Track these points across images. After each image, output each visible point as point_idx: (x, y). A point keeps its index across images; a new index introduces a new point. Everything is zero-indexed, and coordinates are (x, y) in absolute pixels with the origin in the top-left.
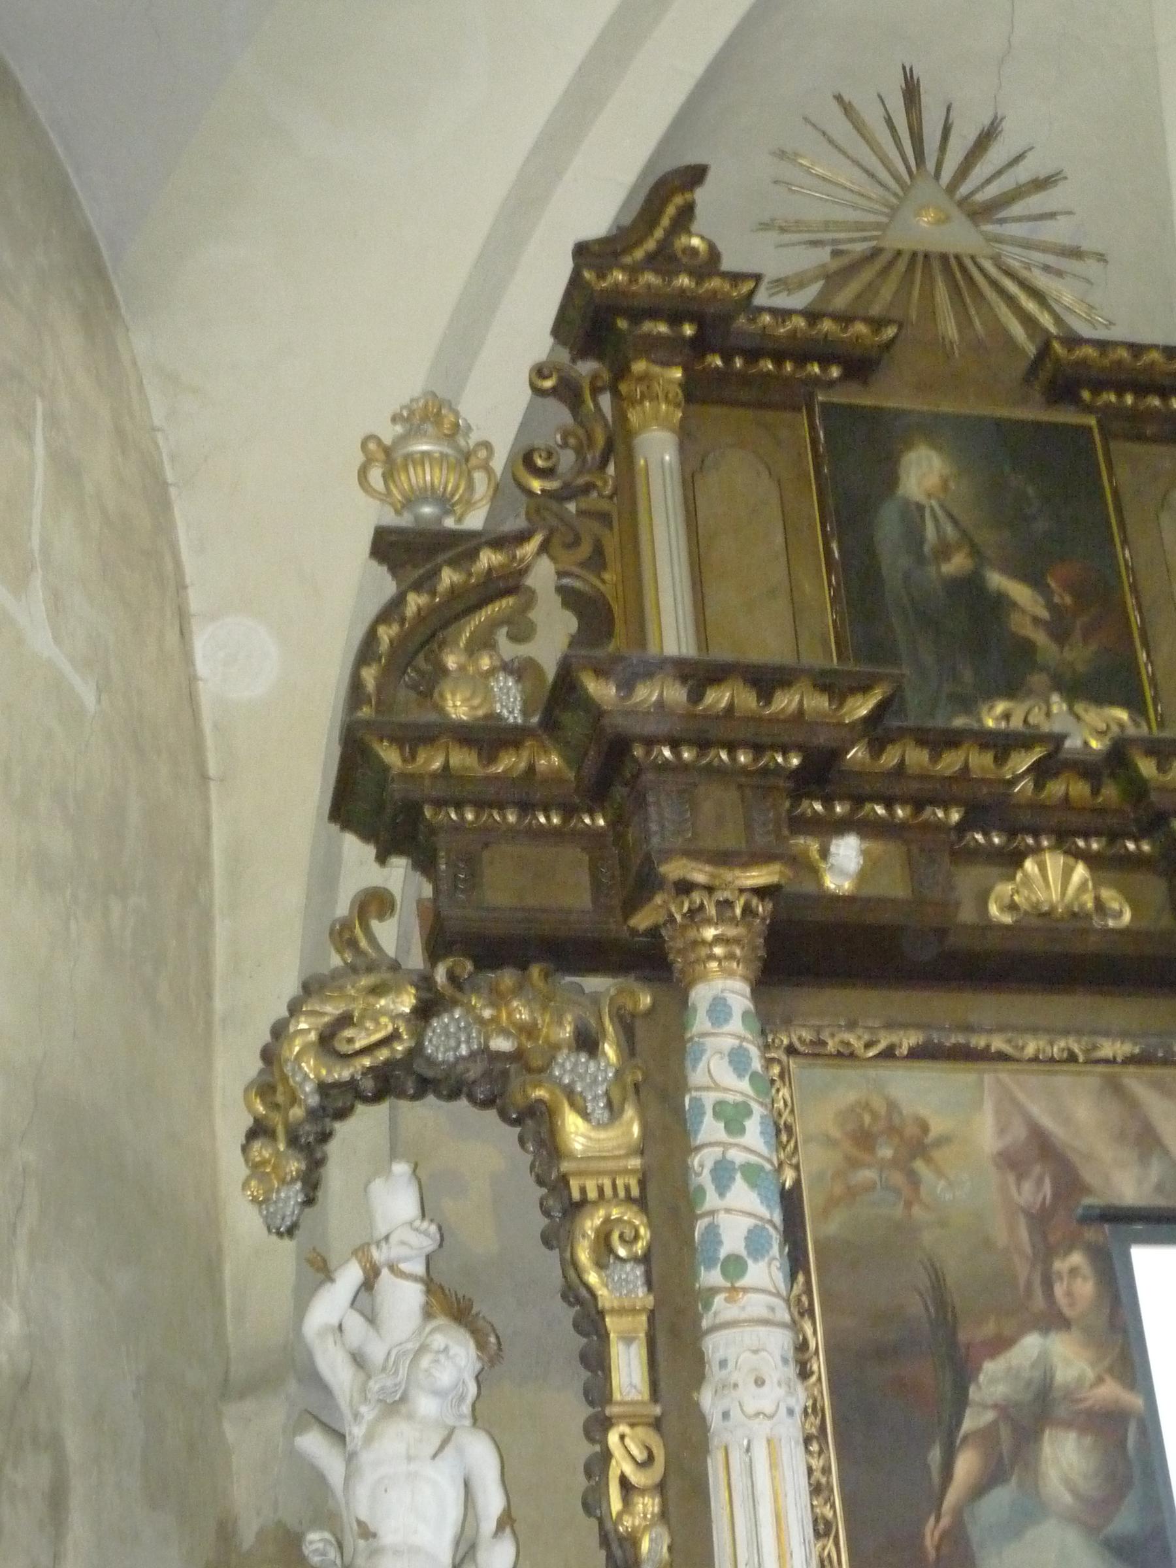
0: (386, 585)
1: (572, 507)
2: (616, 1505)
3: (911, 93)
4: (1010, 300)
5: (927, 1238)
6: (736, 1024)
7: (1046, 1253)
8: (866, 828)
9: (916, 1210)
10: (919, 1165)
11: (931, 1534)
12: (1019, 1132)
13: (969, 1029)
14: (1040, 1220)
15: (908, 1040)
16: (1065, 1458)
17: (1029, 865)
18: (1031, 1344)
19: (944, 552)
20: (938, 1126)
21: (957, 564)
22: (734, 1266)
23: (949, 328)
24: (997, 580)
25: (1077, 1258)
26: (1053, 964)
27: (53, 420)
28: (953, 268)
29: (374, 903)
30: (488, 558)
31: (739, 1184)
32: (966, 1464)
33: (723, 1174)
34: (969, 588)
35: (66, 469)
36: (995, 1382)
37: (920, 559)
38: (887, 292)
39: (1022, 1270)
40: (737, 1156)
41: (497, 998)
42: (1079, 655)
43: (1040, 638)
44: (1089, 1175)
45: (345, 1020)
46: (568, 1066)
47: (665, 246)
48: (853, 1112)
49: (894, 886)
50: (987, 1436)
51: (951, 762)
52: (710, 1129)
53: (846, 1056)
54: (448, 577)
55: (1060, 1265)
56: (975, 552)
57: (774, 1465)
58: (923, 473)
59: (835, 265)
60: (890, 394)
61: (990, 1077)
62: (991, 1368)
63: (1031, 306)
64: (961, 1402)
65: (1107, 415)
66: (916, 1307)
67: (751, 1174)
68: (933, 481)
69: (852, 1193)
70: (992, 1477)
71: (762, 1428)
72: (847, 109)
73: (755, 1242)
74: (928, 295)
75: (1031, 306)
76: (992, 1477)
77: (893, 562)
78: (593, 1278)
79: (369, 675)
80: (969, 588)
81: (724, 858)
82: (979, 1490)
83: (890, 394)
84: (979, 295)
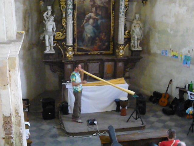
2: (62, 23)
5: (84, 6)
9: (84, 5)
10: (84, 2)
11: (82, 25)
14: (92, 5)
16: (91, 21)
18: (90, 13)
22: (69, 15)
25: (94, 8)
31: (70, 10)
32: (85, 21)
33: (69, 9)
36: (87, 16)
39: (90, 9)
40: (70, 8)
44: (96, 2)
50: (86, 20)
52: (68, 6)
55: (93, 8)
57: (70, 27)
62: (87, 15)
64: (85, 17)
67: (71, 9)
70: (86, 22)
71: (70, 25)
73: (70, 13)
76: (86, 22)
78: (62, 10)
82: (85, 23)
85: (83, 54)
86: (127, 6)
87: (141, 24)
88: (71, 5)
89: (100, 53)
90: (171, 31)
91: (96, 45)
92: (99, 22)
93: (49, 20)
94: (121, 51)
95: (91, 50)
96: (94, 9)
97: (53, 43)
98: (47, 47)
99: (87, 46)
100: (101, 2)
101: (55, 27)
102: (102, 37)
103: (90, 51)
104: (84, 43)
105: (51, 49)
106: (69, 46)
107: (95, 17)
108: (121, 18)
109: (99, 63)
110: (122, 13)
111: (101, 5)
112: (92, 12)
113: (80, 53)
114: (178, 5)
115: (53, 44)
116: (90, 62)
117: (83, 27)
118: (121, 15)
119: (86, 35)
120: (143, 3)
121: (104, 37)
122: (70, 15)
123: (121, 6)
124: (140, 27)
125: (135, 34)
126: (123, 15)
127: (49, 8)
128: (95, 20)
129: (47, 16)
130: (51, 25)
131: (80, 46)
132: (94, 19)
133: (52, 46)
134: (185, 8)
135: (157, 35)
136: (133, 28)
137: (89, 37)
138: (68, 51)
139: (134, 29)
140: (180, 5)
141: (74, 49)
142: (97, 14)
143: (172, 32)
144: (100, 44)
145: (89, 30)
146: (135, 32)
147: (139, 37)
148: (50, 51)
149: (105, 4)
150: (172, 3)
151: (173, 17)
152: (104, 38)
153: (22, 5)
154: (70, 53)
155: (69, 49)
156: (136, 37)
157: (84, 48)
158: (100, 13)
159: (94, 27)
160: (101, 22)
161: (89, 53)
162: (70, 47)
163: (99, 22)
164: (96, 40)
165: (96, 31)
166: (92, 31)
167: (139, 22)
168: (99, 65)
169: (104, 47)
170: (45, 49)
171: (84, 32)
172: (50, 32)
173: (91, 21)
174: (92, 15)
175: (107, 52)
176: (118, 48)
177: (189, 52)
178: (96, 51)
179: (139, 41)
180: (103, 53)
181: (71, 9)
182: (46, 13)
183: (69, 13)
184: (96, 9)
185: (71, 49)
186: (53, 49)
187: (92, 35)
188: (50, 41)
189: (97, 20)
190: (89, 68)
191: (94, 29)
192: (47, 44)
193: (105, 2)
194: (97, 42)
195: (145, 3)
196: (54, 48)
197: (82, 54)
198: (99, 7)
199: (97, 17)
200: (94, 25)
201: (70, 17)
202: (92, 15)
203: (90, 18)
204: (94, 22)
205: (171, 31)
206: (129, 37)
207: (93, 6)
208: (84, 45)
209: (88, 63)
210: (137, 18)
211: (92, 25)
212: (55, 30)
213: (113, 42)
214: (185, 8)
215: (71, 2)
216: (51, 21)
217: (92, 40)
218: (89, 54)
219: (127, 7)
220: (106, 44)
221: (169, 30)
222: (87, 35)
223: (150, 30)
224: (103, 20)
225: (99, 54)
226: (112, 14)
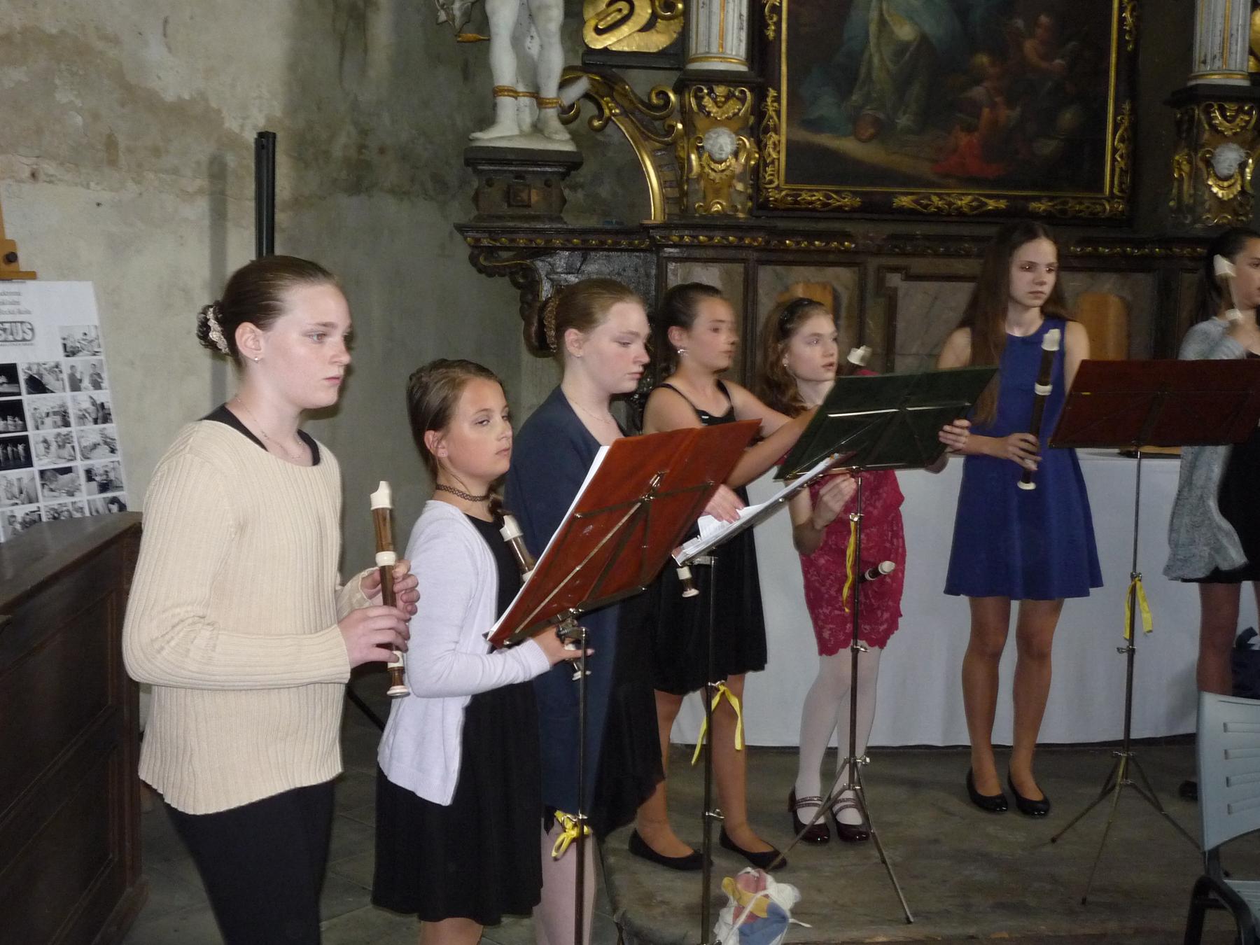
89: (1002, 204)
91: (970, 129)
94: (1228, 157)
95: (924, 169)
98: (498, 92)
99: (883, 131)
102: (1029, 46)
103: (908, 181)
104: (855, 98)
106: (713, 79)
113: (814, 195)
115: (563, 85)
116: (919, 265)
119: (873, 28)
131: (815, 125)
133: (550, 90)
137: (902, 48)
138: (700, 122)
141: (759, 112)
144: (1009, 115)
148: (522, 134)
152: (1044, 65)
154: (723, 142)
155: (707, 102)
157: (848, 145)
161: (905, 201)
162: (720, 90)
169: (1048, 147)
170: (487, 119)
175: (1078, 203)
176: (1189, 136)
186: (555, 124)
188: (533, 47)
190: (900, 325)
192: (505, 67)
194: (978, 92)
197: (836, 201)
208: (853, 123)
209: (895, 280)
213: (1127, 106)
218: (901, 210)
220: (1068, 118)
222: (883, 23)
225: (997, 213)
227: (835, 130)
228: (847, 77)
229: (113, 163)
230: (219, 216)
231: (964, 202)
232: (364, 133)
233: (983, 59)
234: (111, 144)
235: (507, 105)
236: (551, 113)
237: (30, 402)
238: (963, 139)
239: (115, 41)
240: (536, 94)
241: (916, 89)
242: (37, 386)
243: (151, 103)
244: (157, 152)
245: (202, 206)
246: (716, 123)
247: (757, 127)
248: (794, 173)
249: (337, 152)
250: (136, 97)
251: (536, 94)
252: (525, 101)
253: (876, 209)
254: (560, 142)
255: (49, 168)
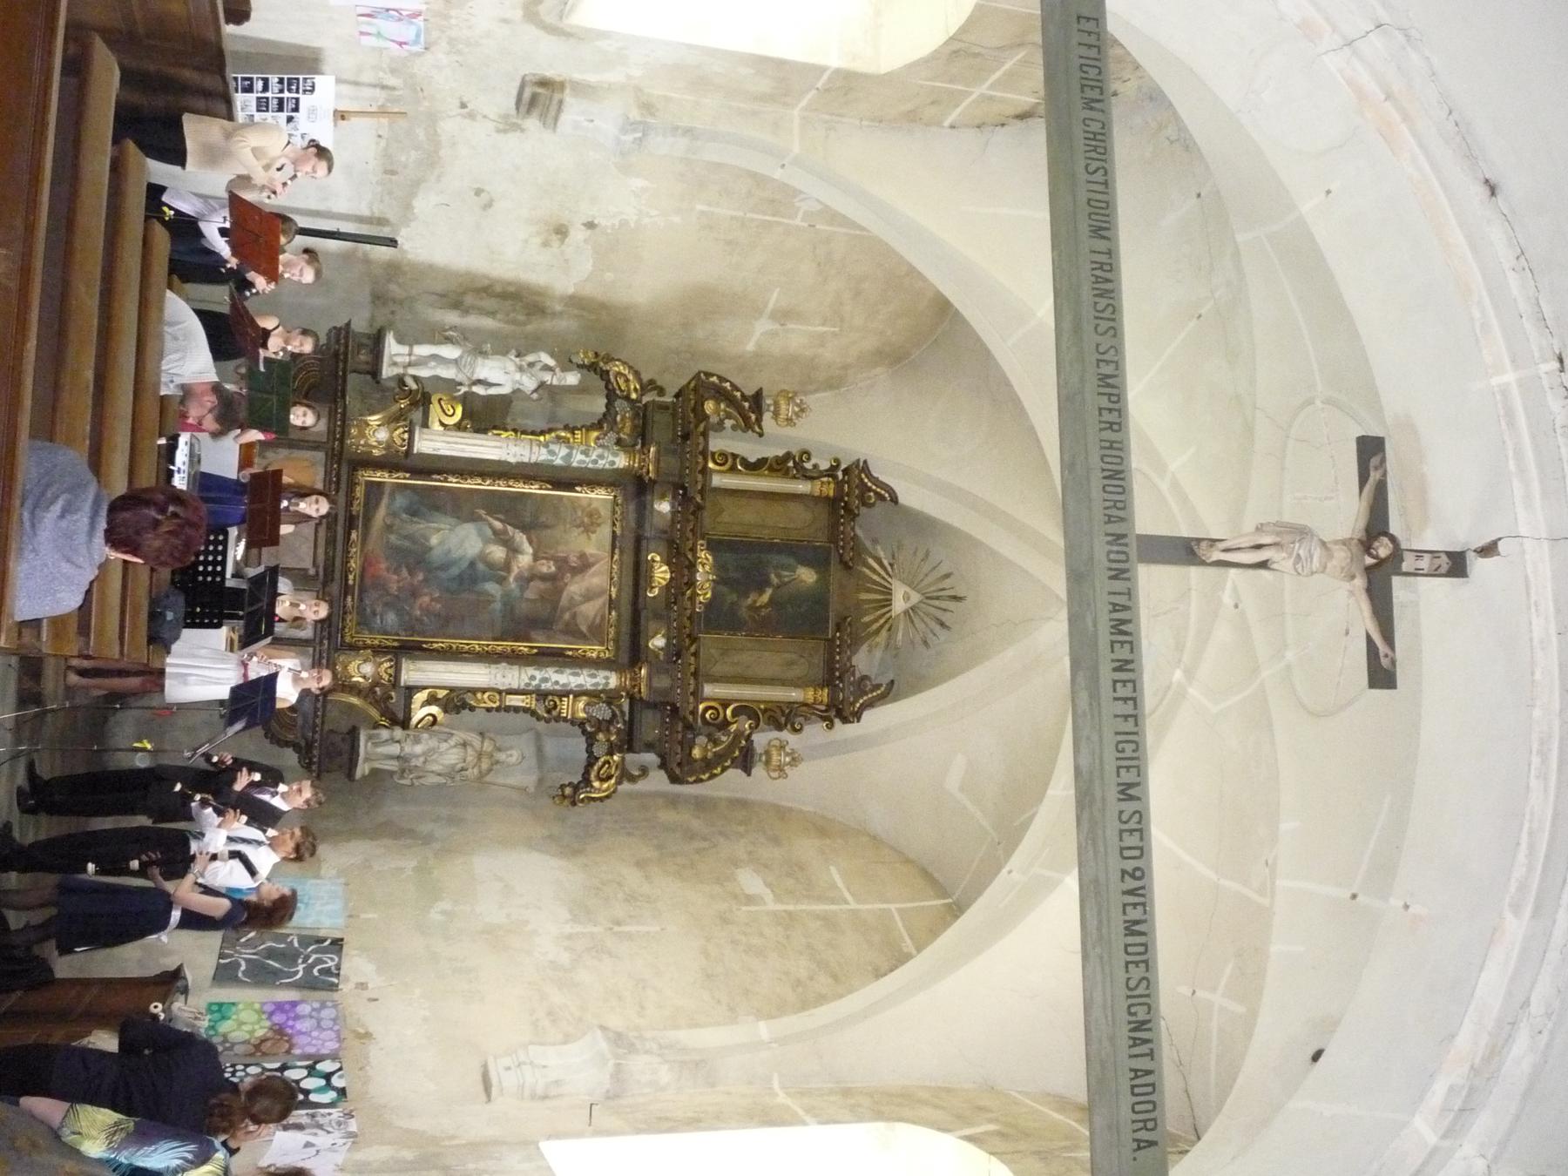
0: (749, 392)
1: (791, 464)
3: (955, 598)
4: (876, 620)
6: (611, 458)
7: (556, 560)
8: (674, 513)
11: (482, 512)
12: (591, 560)
13: (621, 553)
14: (565, 560)
15: (618, 532)
16: (498, 553)
17: (665, 568)
18: (530, 550)
19: (779, 576)
20: (593, 536)
21: (775, 580)
23: (864, 596)
24: (769, 592)
26: (639, 573)
27: (834, 334)
28: (887, 603)
29: (661, 391)
30: (753, 417)
32: (498, 525)
34: (767, 583)
35: (821, 340)
36: (520, 538)
37: (776, 567)
38: (875, 577)
41: (633, 419)
42: (744, 613)
43: (749, 601)
44: (578, 578)
45: (627, 381)
46: (612, 436)
47: (870, 490)
48: (598, 512)
49: (656, 521)
50: (505, 532)
51: (690, 535)
53: (614, 512)
54: (747, 405)
56: (779, 587)
58: (807, 576)
59: (886, 562)
60: (835, 569)
61: (607, 555)
63: (875, 627)
64: (516, 527)
65: (832, 641)
66: (543, 519)
67: (569, 455)
68: (804, 577)
69: (574, 509)
70: (495, 532)
72: (947, 576)
73: (552, 453)
74: (876, 592)
75: (875, 627)
76: (495, 532)
77: (776, 559)
79: (714, 379)
80: (767, 583)
81: (658, 461)
82: (491, 527)
83: (835, 569)
84: (877, 609)
85: (355, 509)
86: (554, 713)
87: (476, 771)
88: (582, 457)
90: (444, 912)
91: (388, 570)
92: (492, 588)
93: (521, 369)
94: (368, 669)
96: (547, 568)
97: (424, 373)
98: (411, 346)
99: (389, 528)
100: (577, 598)
101: (493, 391)
102: (426, 599)
105: (395, 364)
106: (411, 432)
107: (515, 570)
108: (516, 673)
109: (312, 572)
110: (539, 674)
111: (564, 601)
112: (536, 558)
113: (360, 492)
114: (568, 929)
117: (473, 518)
118: (531, 671)
120: (562, 787)
121: (427, 611)
122: (544, 450)
123: (568, 671)
124: (463, 769)
125: (433, 743)
126: (533, 678)
127: (572, 379)
128: (499, 572)
129: (538, 366)
130: (500, 375)
132: (507, 566)
133: (411, 371)
134: (565, 958)
135: (409, 863)
136: (460, 736)
139: (452, 742)
140: (570, 937)
142: (527, 579)
143: (435, 915)
144: (394, 588)
145: (461, 540)
146: (444, 746)
147: (419, 762)
149: (567, 616)
150: (570, 911)
151: (508, 916)
153: (571, 290)
154: (383, 435)
156: (418, 749)
157: (381, 514)
158: (530, 594)
159: (472, 564)
160: (490, 599)
161: (354, 535)
162: (406, 436)
163: (492, 588)
164: (411, 573)
165: (455, 571)
166: (456, 555)
167: (485, 765)
168: (305, 570)
170: (400, 341)
171: (452, 521)
172: (472, 366)
173: (498, 553)
174: (525, 560)
177: (362, 986)
178: (363, 570)
179: (392, 766)
180: (349, 599)
181: (569, 455)
182: (551, 362)
183: (552, 447)
184: (544, 578)
185: (399, 442)
187: (436, 555)
189: (501, 581)
191: (465, 565)
192: (423, 350)
193: (574, 616)
194: (405, 573)
195: (564, 797)
196: (401, 381)
198: (559, 592)
199: (516, 579)
200: (481, 566)
201: (535, 449)
202: (525, 560)
203: (514, 550)
204: (491, 565)
205: (444, 912)
206: (414, 720)
207: (562, 563)
210: (501, 756)
211: (483, 557)
212: (480, 390)
214: (565, 958)
215: (595, 462)
216: (518, 376)
217: (415, 557)
219: (549, 711)
221: (444, 905)
222: (439, 530)
223: (427, 840)
224: (498, 606)
226: (523, 647)
227: (388, 507)
228: (413, 512)
229: (386, 172)
230: (360, 219)
231: (352, 564)
232: (401, 303)
233: (421, 577)
234: (393, 173)
235: (405, 349)
236: (401, 371)
237: (283, 116)
238: (383, 566)
239: (439, 179)
240: (410, 364)
241: (407, 544)
242: (290, 119)
243: (413, 195)
244: (390, 193)
245: (366, 212)
246: (392, 433)
247: (390, 463)
248: (370, 484)
249: (393, 287)
250: (415, 185)
251: (410, 364)
252: (407, 359)
253: (351, 522)
254: (387, 371)
255: (383, 143)
